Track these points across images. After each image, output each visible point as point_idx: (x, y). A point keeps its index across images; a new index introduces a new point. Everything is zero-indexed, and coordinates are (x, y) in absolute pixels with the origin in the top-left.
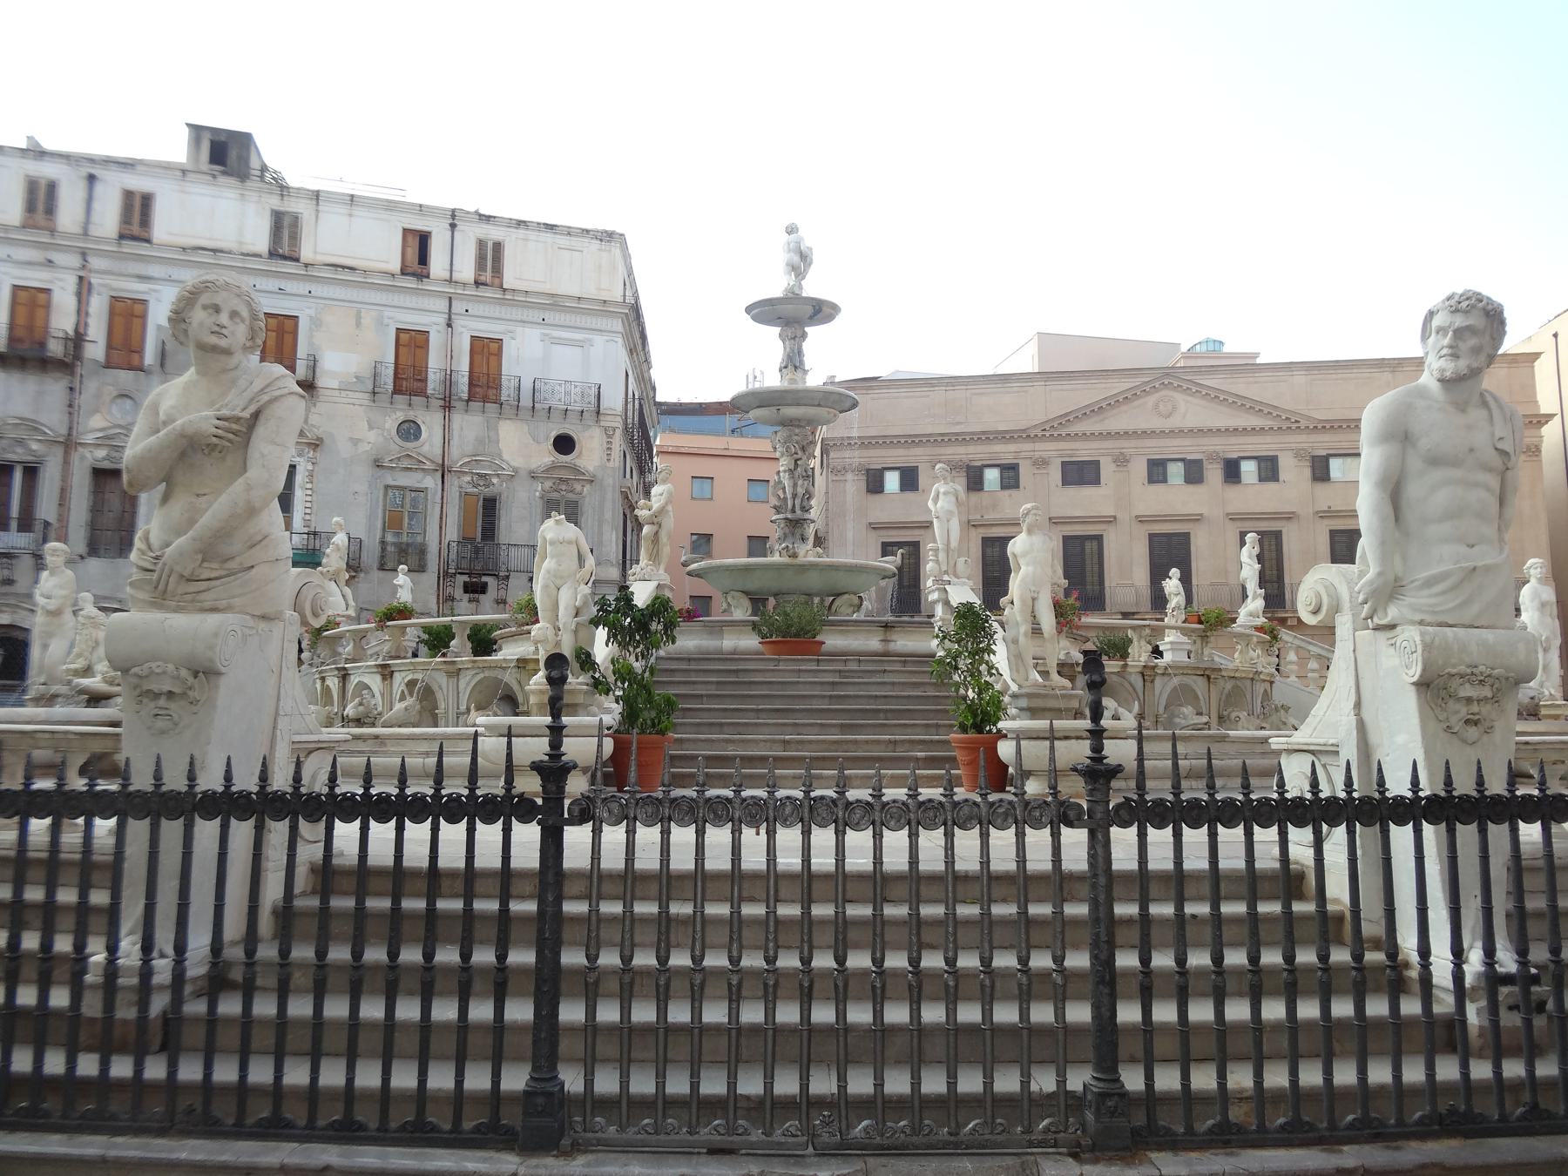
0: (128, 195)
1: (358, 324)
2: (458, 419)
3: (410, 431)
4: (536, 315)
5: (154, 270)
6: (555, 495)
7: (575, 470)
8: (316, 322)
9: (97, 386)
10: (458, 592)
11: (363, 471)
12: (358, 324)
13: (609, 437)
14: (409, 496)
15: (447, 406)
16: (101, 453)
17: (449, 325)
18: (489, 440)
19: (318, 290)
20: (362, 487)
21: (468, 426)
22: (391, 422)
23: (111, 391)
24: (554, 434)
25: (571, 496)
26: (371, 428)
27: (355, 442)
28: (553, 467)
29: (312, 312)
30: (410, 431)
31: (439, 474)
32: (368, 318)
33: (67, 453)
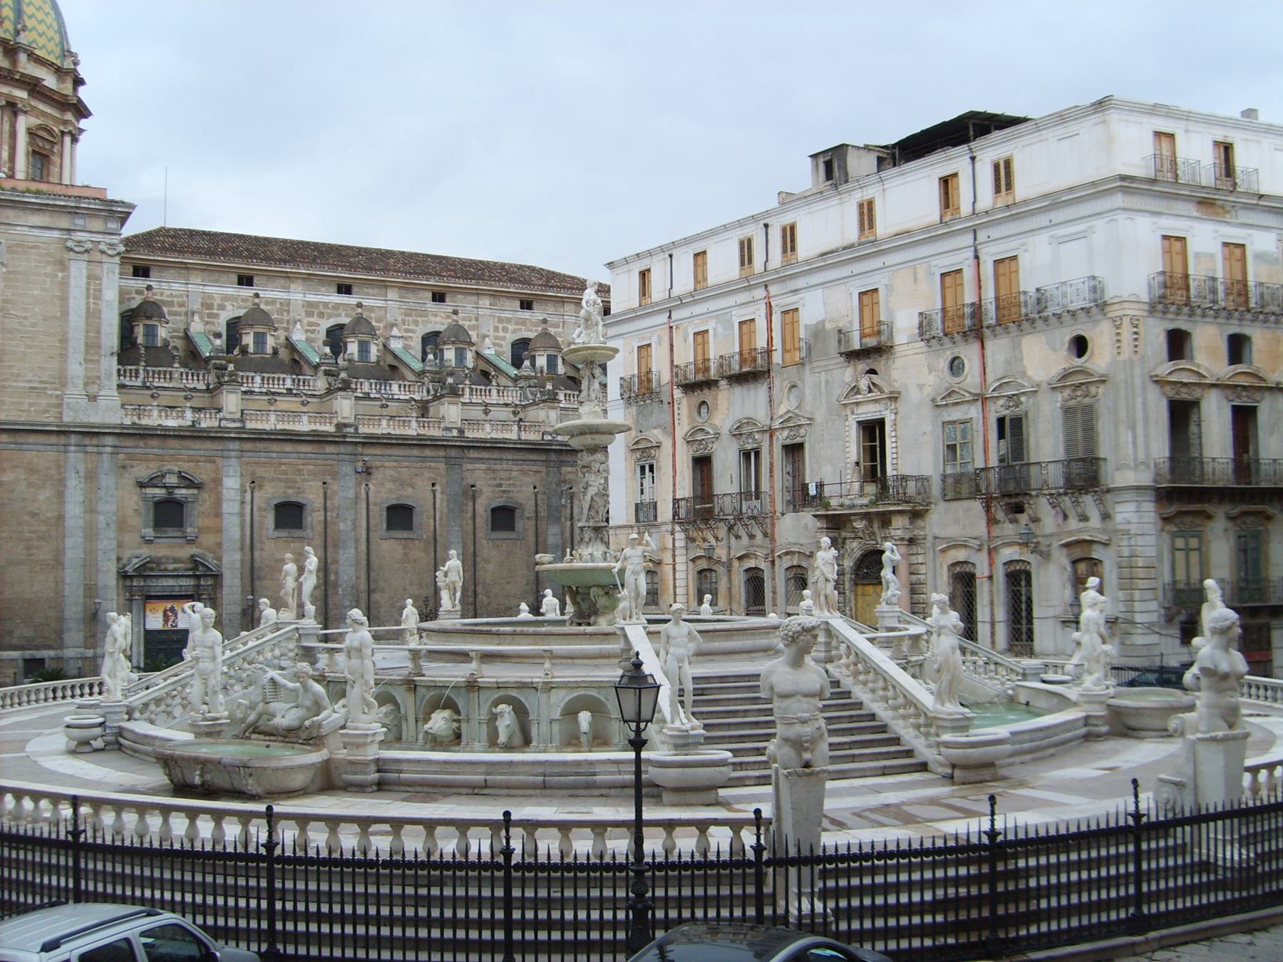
1: (916, 280)
3: (956, 366)
4: (1042, 220)
5: (800, 283)
6: (1073, 403)
7: (1082, 371)
8: (890, 288)
10: (1000, 515)
11: (927, 411)
12: (916, 280)
13: (1118, 327)
14: (959, 427)
16: (786, 433)
17: (977, 257)
18: (1015, 359)
19: (891, 259)
20: (927, 427)
21: (997, 348)
22: (943, 364)
23: (787, 384)
24: (1068, 338)
25: (1087, 401)
26: (930, 371)
27: (921, 387)
28: (1066, 375)
29: (885, 281)
30: (956, 366)
31: (979, 403)
32: (921, 274)
33: (771, 436)
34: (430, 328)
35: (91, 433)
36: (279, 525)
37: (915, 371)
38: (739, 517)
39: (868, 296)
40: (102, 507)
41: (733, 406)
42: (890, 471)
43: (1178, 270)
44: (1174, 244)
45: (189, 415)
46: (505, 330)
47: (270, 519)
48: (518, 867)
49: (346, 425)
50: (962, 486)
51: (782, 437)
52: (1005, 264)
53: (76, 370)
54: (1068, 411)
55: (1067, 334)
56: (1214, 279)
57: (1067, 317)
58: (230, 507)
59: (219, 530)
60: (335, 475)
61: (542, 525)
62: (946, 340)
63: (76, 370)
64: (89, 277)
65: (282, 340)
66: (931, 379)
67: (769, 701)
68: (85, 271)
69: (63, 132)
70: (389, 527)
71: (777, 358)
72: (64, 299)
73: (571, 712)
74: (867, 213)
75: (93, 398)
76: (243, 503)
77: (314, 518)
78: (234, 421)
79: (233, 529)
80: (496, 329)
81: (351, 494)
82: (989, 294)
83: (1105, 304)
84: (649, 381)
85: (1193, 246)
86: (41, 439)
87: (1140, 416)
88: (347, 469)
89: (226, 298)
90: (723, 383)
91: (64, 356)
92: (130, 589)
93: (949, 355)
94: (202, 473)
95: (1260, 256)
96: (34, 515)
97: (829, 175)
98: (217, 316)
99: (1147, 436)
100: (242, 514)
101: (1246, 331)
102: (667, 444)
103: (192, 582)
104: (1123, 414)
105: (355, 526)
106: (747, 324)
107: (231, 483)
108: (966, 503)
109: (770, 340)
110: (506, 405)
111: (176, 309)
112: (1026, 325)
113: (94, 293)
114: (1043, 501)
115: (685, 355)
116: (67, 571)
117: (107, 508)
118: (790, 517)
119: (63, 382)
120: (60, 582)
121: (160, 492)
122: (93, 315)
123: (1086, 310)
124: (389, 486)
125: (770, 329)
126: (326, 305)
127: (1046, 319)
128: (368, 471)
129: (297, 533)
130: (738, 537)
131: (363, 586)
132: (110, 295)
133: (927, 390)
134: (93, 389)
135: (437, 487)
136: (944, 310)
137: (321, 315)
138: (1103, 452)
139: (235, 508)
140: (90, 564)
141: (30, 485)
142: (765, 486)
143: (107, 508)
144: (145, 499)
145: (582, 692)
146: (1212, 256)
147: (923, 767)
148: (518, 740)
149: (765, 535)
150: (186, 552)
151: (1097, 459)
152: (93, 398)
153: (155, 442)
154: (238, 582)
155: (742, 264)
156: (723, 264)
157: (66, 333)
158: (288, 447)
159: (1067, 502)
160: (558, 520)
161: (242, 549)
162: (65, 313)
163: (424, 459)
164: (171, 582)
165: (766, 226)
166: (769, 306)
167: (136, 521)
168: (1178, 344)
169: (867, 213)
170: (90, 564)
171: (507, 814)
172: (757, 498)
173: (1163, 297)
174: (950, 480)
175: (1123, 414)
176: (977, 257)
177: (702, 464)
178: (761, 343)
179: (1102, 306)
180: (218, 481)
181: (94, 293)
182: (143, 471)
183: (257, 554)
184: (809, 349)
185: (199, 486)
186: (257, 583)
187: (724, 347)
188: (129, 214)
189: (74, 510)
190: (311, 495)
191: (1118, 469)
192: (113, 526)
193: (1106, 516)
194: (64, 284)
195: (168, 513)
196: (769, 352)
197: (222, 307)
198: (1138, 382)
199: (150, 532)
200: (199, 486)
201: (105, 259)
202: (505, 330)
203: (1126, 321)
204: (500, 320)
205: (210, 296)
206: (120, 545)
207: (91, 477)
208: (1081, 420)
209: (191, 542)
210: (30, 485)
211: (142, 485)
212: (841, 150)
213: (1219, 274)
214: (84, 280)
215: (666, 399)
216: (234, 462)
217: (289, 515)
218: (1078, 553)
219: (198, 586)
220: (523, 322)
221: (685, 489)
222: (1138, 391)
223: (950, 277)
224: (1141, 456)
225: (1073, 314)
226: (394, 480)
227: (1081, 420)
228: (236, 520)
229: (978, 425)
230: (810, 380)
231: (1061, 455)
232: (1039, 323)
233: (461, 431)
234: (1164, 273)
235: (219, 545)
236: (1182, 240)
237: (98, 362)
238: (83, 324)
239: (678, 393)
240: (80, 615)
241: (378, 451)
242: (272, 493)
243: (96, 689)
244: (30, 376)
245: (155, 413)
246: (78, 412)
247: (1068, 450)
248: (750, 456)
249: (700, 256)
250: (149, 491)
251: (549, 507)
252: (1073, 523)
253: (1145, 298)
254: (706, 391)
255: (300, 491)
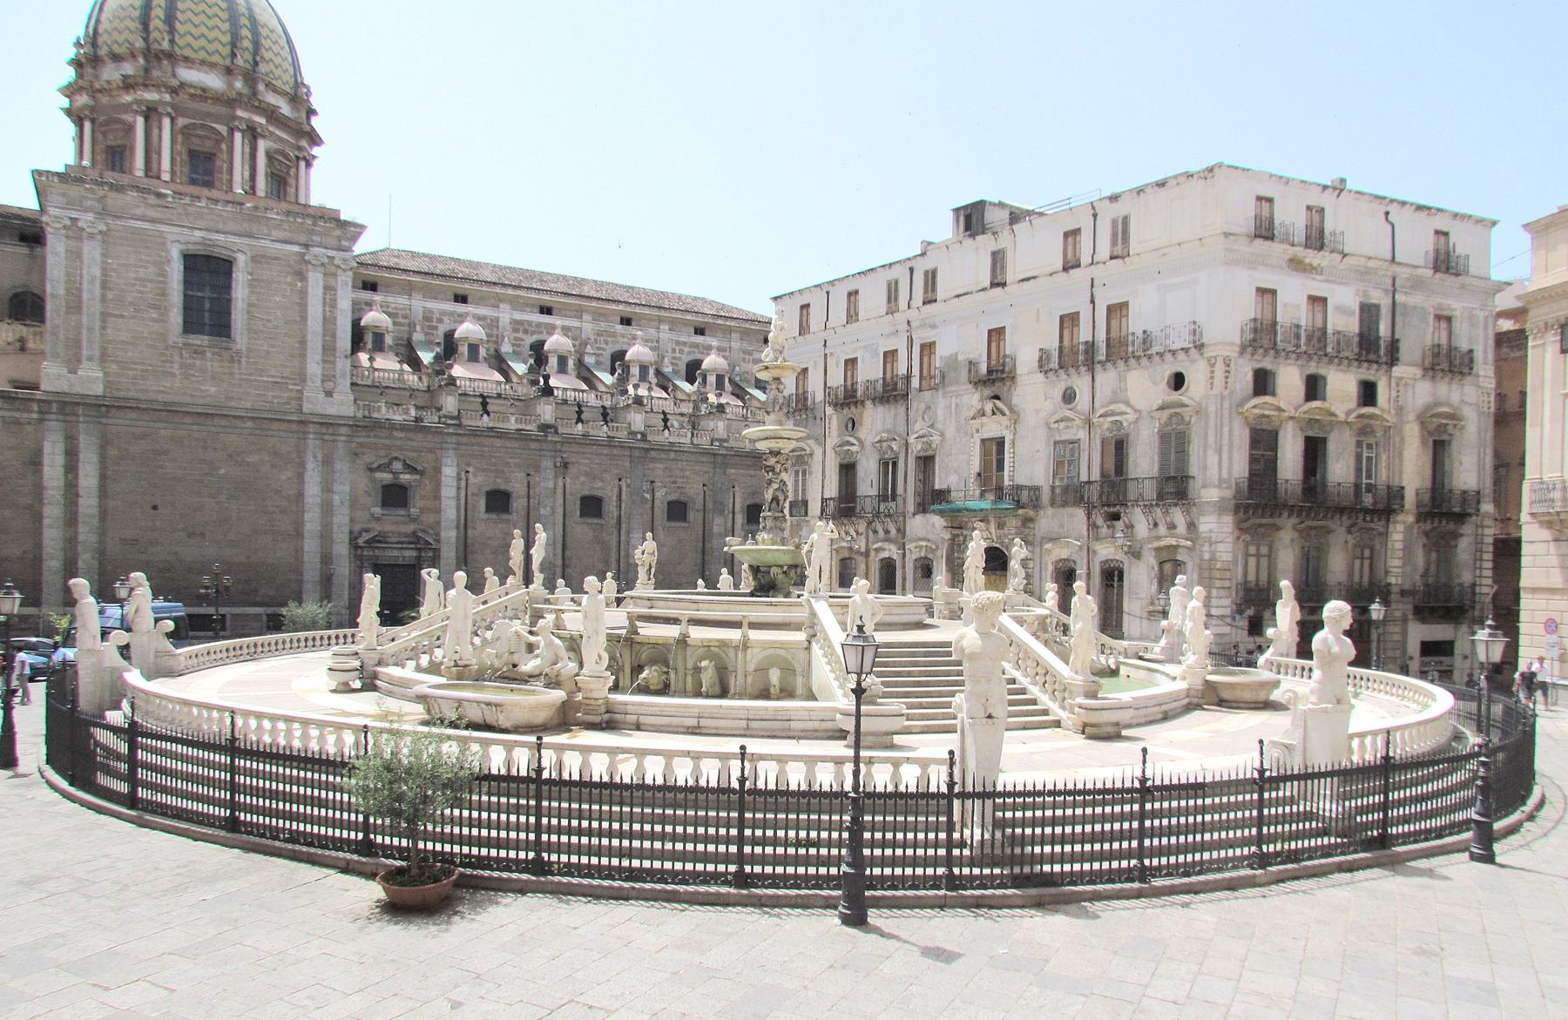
0: (926, 273)
2: (1100, 376)
3: (1069, 397)
9: (917, 404)
10: (1100, 521)
11: (1042, 432)
15: (1092, 371)
17: (1092, 302)
21: (1106, 379)
22: (1057, 393)
24: (1168, 373)
27: (1037, 411)
30: (1069, 397)
34: (617, 348)
35: (328, 424)
36: (489, 509)
37: (1034, 394)
38: (877, 515)
39: (996, 335)
40: (336, 487)
41: (876, 421)
42: (1007, 482)
43: (1268, 316)
44: (1266, 293)
45: (413, 412)
46: (681, 351)
47: (482, 504)
48: (750, 792)
49: (549, 426)
50: (1072, 494)
51: (916, 447)
52: (1117, 310)
53: (314, 368)
54: (1164, 437)
55: (1168, 369)
56: (1298, 326)
57: (1168, 357)
58: (448, 491)
59: (438, 511)
60: (537, 468)
61: (709, 516)
62: (1062, 372)
63: (314, 368)
64: (325, 288)
65: (492, 351)
66: (1047, 406)
67: (959, 663)
68: (321, 283)
69: (298, 158)
70: (582, 515)
71: (915, 383)
72: (303, 307)
73: (762, 670)
74: (998, 259)
75: (329, 394)
76: (459, 488)
77: (518, 504)
78: (452, 418)
79: (450, 512)
80: (674, 351)
81: (551, 485)
82: (1101, 335)
83: (1203, 345)
84: (806, 399)
85: (1281, 298)
86: (284, 426)
87: (1226, 442)
88: (547, 463)
89: (443, 313)
90: (868, 403)
91: (303, 356)
92: (360, 558)
93: (1062, 386)
94: (425, 462)
95: (1340, 309)
96: (277, 492)
97: (968, 227)
98: (436, 328)
99: (1230, 458)
100: (458, 499)
101: (1322, 372)
102: (818, 451)
103: (414, 554)
104: (1211, 440)
105: (553, 512)
106: (890, 356)
107: (449, 472)
108: (1070, 510)
109: (910, 368)
110: (682, 415)
111: (400, 320)
112: (1132, 362)
113: (330, 302)
114: (1138, 511)
115: (837, 379)
116: (307, 541)
117: (342, 490)
118: (919, 518)
119: (302, 377)
120: (299, 551)
121: (386, 477)
122: (329, 322)
123: (1186, 350)
124: (583, 479)
125: (910, 359)
126: (530, 323)
127: (1150, 357)
128: (565, 465)
129: (505, 516)
130: (875, 532)
131: (559, 562)
132: (344, 303)
133: (1043, 414)
134: (329, 385)
135: (623, 483)
136: (1061, 348)
137: (526, 332)
138: (1193, 470)
139: (453, 492)
140: (326, 536)
141: (273, 466)
142: (900, 490)
143: (342, 490)
144: (373, 481)
145: (771, 651)
146: (1298, 306)
147: (1057, 724)
148: (717, 690)
149: (899, 530)
150: (411, 527)
151: (1187, 477)
152: (329, 394)
153: (384, 433)
154: (453, 554)
155: (889, 301)
156: (873, 301)
157: (304, 336)
158: (498, 443)
159: (1158, 512)
160: (722, 513)
161: (458, 528)
162: (304, 318)
163: (612, 457)
164: (396, 553)
165: (911, 270)
166: (911, 341)
167: (367, 500)
168: (1263, 383)
169: (998, 259)
170: (326, 536)
171: (743, 747)
172: (894, 499)
173: (1254, 340)
174: (1058, 491)
175: (1211, 440)
176: (1092, 302)
177: (848, 470)
178: (902, 369)
179: (1200, 347)
180: (438, 470)
181: (330, 302)
182: (369, 458)
183: (470, 532)
184: (943, 377)
185: (422, 473)
186: (470, 556)
187: (870, 372)
188: (360, 234)
189: (312, 489)
190: (517, 485)
191: (1204, 487)
192: (347, 504)
193: (1191, 526)
194: (303, 293)
195: (395, 496)
196: (908, 378)
197: (440, 321)
198: (1226, 413)
199: (378, 510)
200: (422, 473)
201: (339, 272)
202: (681, 351)
203: (1220, 360)
204: (678, 343)
205: (431, 311)
206: (352, 521)
207: (327, 462)
208: (1175, 442)
209: (413, 520)
210: (273, 466)
211: (371, 470)
212: (979, 206)
213: (1303, 323)
214: (321, 290)
215: (819, 414)
216: (451, 453)
217: (498, 501)
218: (1165, 556)
219: (419, 558)
220: (696, 346)
221: (832, 491)
222: (1226, 421)
223: (1069, 321)
224: (1225, 475)
225: (1174, 353)
226: (587, 474)
227: (1175, 442)
228: (453, 503)
229: (1084, 446)
230: (942, 404)
231: (1155, 471)
232: (1144, 361)
233: (644, 435)
234: (1255, 320)
235: (438, 523)
236: (1273, 292)
237: (334, 363)
238: (320, 329)
239: (829, 410)
240: (317, 579)
241: (575, 448)
242: (480, 481)
243: (350, 640)
244: (273, 372)
245: (384, 409)
246: (315, 402)
247: (1161, 468)
248: (888, 466)
249: (853, 294)
250: (379, 475)
251: (715, 502)
252: (1162, 530)
253: (1238, 341)
254: (853, 409)
255: (507, 481)
